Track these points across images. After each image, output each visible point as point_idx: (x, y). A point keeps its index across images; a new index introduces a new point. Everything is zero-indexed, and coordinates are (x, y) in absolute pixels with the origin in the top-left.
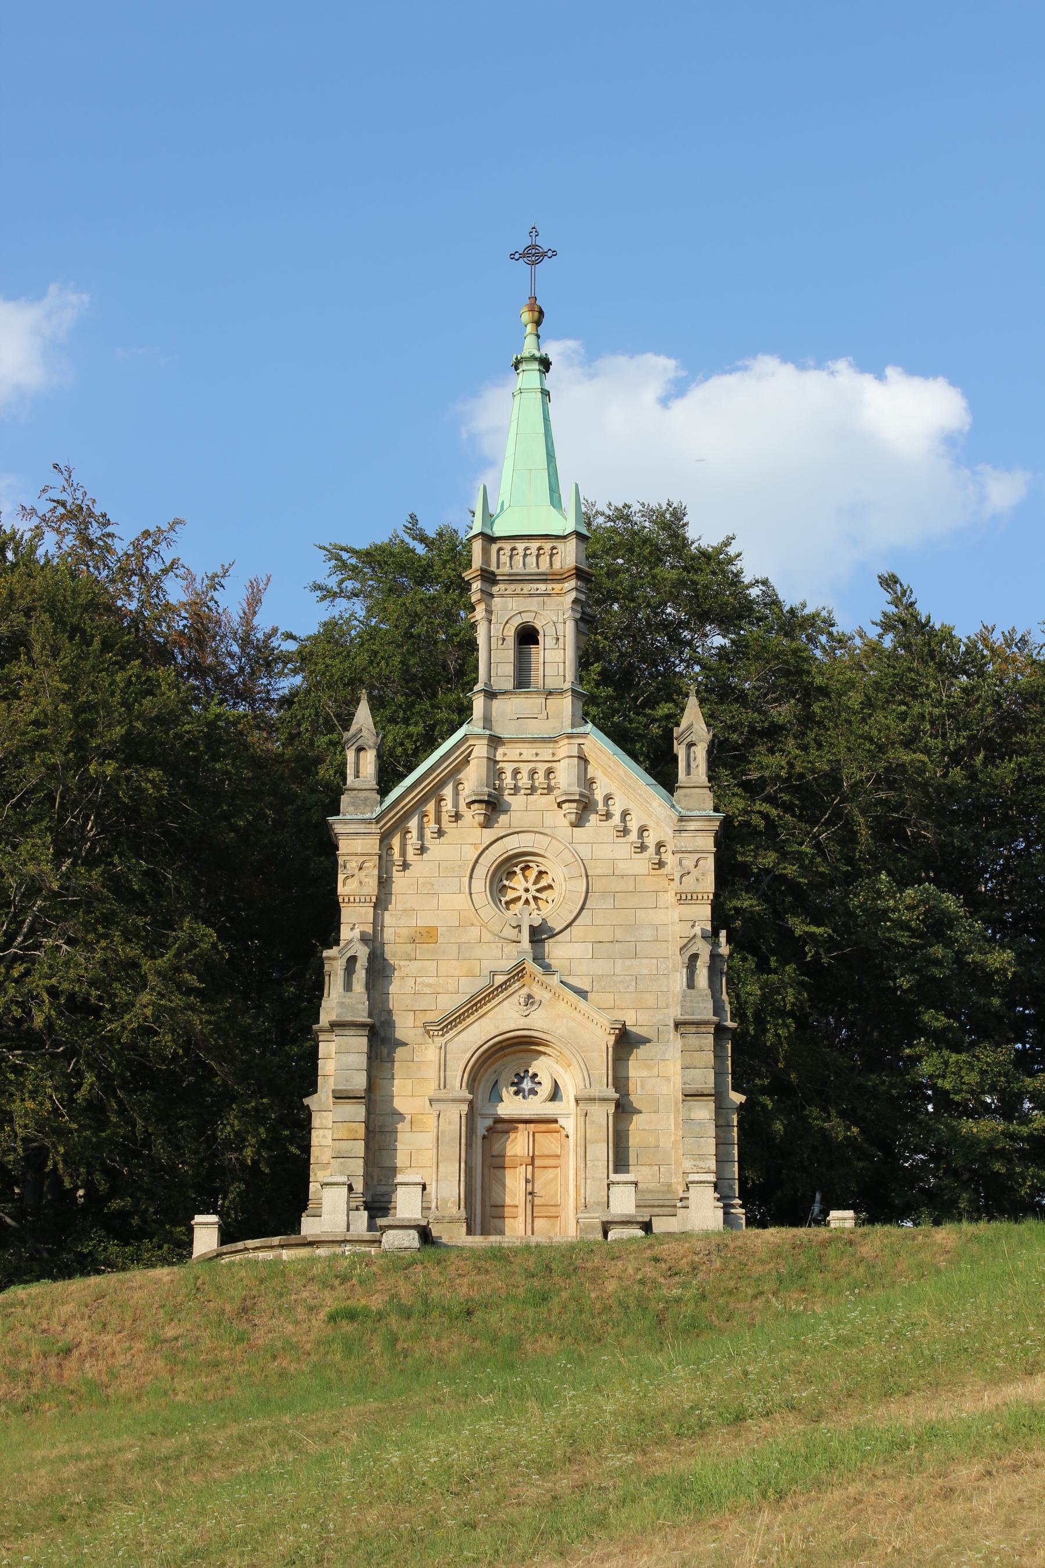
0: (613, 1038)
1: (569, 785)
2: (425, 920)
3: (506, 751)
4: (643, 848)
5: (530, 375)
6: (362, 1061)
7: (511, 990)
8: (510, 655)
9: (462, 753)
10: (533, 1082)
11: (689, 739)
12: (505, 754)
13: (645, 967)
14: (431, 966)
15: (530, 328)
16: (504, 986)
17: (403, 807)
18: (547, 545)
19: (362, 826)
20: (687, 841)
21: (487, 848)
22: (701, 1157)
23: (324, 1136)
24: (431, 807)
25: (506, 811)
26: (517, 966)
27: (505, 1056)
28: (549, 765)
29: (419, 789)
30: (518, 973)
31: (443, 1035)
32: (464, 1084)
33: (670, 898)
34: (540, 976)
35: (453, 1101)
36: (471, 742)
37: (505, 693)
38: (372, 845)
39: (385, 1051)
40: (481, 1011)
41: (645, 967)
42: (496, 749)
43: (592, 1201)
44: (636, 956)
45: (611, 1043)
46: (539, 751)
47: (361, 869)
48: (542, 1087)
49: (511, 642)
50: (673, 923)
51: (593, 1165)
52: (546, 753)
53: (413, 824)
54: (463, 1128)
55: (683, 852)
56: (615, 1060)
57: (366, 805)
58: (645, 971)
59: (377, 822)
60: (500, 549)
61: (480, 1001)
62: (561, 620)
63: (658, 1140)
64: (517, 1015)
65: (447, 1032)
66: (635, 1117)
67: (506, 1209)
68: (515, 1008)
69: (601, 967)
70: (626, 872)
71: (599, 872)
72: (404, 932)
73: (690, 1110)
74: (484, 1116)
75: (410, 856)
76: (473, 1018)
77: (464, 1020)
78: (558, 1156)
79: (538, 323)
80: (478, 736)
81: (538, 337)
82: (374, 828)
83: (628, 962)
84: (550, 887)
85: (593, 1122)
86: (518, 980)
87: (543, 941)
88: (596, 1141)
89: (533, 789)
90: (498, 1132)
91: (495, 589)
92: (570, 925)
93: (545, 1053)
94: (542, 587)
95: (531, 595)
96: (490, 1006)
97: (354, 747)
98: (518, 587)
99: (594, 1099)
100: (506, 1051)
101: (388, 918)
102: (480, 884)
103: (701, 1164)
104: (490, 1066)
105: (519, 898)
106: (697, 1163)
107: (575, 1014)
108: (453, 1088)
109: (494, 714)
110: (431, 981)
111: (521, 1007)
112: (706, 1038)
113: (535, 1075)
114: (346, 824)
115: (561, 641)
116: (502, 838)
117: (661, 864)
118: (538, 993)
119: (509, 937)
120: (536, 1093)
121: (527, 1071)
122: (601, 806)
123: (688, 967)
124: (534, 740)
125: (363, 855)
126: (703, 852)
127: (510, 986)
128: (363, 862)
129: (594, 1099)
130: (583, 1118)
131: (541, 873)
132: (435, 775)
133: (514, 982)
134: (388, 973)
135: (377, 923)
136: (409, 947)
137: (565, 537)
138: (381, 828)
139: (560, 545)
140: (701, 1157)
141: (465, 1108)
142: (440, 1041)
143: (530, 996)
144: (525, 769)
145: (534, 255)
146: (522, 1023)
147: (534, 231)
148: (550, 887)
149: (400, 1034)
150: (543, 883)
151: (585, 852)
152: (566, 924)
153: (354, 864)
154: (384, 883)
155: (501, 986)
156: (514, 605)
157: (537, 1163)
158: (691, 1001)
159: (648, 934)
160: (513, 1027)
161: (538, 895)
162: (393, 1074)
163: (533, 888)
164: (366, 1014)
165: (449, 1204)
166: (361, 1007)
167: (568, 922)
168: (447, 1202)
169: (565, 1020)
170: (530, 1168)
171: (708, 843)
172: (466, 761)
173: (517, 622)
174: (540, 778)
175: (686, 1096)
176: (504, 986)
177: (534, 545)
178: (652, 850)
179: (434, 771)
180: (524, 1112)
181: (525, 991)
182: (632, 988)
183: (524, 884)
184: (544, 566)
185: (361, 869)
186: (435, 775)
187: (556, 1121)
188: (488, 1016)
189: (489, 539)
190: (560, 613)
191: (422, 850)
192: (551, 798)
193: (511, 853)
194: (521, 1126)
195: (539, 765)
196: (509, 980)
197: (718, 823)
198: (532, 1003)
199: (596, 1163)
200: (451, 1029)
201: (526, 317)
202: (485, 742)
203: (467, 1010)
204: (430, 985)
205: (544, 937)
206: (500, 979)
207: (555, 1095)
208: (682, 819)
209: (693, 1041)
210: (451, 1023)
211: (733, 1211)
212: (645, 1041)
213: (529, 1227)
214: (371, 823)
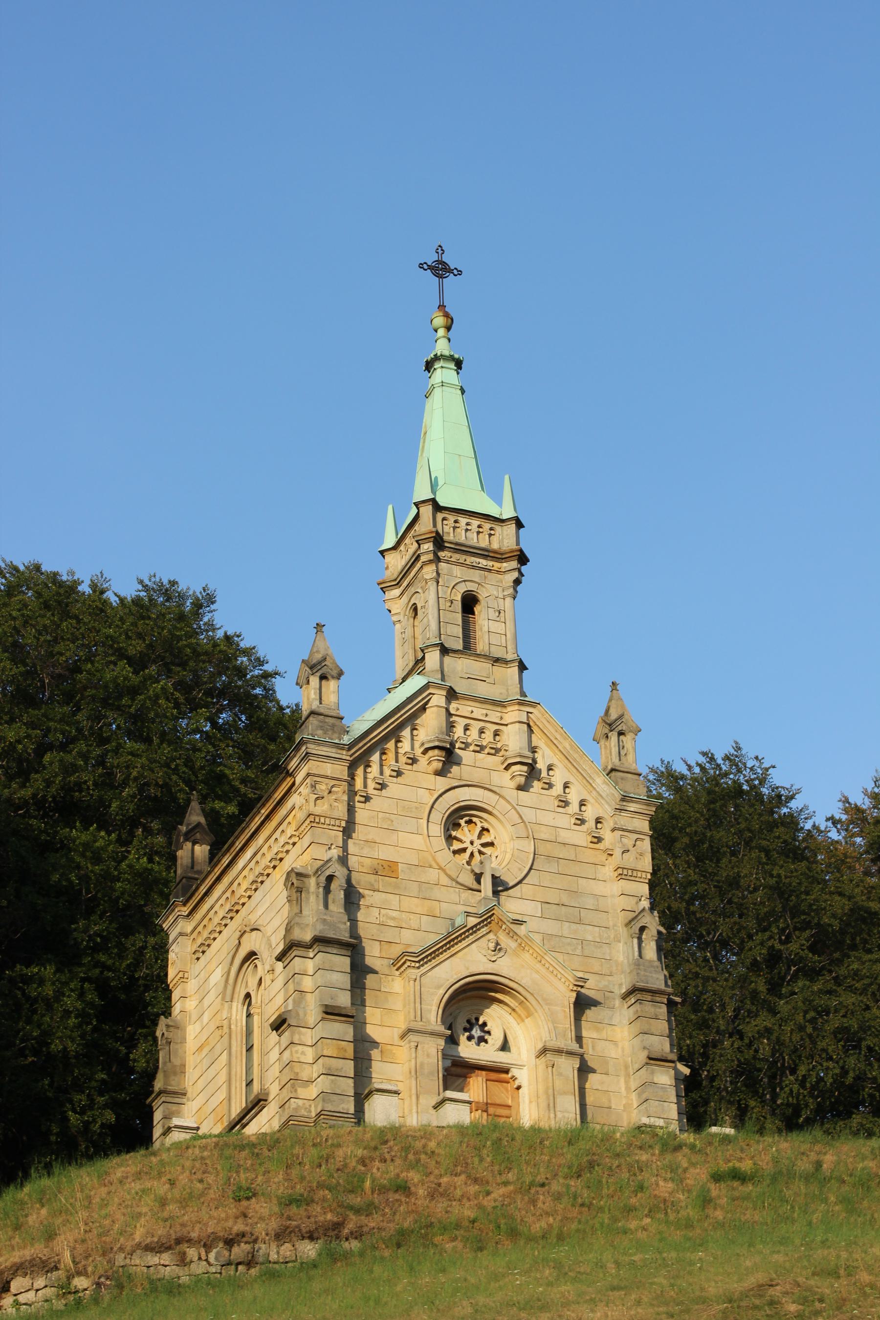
0: (574, 995)
1: (520, 748)
2: (385, 854)
3: (460, 707)
4: (582, 822)
5: (444, 373)
6: (344, 980)
7: (480, 933)
8: (459, 617)
9: (423, 699)
10: (483, 1031)
11: (620, 728)
13: (590, 933)
14: (394, 900)
15: (441, 332)
16: (474, 929)
18: (487, 526)
19: (334, 750)
21: (441, 796)
23: (303, 1053)
24: (391, 745)
25: (459, 764)
26: (489, 911)
28: (497, 727)
29: (386, 725)
30: (487, 919)
31: (418, 968)
32: (439, 1019)
33: (608, 871)
34: (508, 924)
36: (431, 691)
37: (455, 651)
38: (341, 771)
41: (590, 933)
44: (580, 922)
46: (489, 712)
47: (330, 792)
49: (458, 606)
50: (613, 896)
52: (494, 716)
53: (375, 757)
55: (623, 830)
56: (575, 1019)
57: (334, 732)
58: (590, 938)
59: (349, 749)
60: (444, 519)
61: (453, 940)
62: (501, 596)
63: (610, 1101)
64: (485, 960)
66: (591, 1076)
68: (484, 952)
70: (567, 841)
71: (543, 836)
72: (367, 862)
73: (653, 1073)
78: (509, 1107)
79: (448, 328)
80: (438, 686)
81: (449, 340)
82: (345, 755)
83: (574, 926)
84: (492, 844)
85: (560, 1074)
86: (486, 925)
88: (565, 1093)
89: (481, 749)
91: (441, 554)
92: (520, 882)
93: (500, 1002)
94: (483, 562)
95: (473, 567)
97: (318, 674)
98: (462, 558)
100: (469, 994)
102: (437, 829)
105: (464, 850)
107: (538, 966)
108: (429, 1021)
110: (394, 914)
111: (490, 952)
112: (660, 1008)
113: (485, 1024)
114: (319, 745)
115: (502, 614)
117: (599, 840)
118: (506, 941)
119: (466, 884)
120: (486, 1042)
121: (477, 1019)
122: (544, 774)
127: (479, 929)
128: (332, 787)
129: (562, 1052)
131: (484, 829)
132: (399, 715)
133: (483, 927)
135: (345, 848)
136: (372, 878)
137: (503, 521)
138: (351, 756)
139: (498, 529)
142: (414, 973)
143: (497, 944)
144: (475, 726)
145: (441, 269)
146: (490, 967)
147: (440, 249)
148: (492, 844)
149: (369, 961)
150: (486, 839)
151: (529, 815)
153: (323, 787)
154: (351, 810)
155: (472, 928)
156: (457, 571)
157: (491, 1110)
158: (645, 970)
159: (590, 903)
160: (482, 970)
161: (482, 849)
163: (477, 843)
164: (347, 935)
166: (342, 926)
171: (644, 825)
172: (423, 709)
173: (462, 588)
174: (488, 737)
175: (651, 1059)
176: (474, 929)
177: (475, 523)
178: (591, 824)
179: (399, 711)
180: (481, 1058)
181: (491, 936)
182: (578, 952)
183: (475, 837)
184: (484, 542)
185: (330, 792)
186: (399, 715)
187: (507, 1071)
189: (437, 508)
190: (500, 589)
192: (497, 759)
193: (462, 804)
195: (488, 725)
196: (479, 923)
197: (654, 809)
198: (500, 950)
201: (439, 321)
202: (444, 693)
203: (442, 947)
204: (393, 919)
206: (472, 921)
207: (505, 1047)
208: (624, 799)
209: (649, 1008)
210: (427, 957)
212: (594, 1003)
214: (342, 749)
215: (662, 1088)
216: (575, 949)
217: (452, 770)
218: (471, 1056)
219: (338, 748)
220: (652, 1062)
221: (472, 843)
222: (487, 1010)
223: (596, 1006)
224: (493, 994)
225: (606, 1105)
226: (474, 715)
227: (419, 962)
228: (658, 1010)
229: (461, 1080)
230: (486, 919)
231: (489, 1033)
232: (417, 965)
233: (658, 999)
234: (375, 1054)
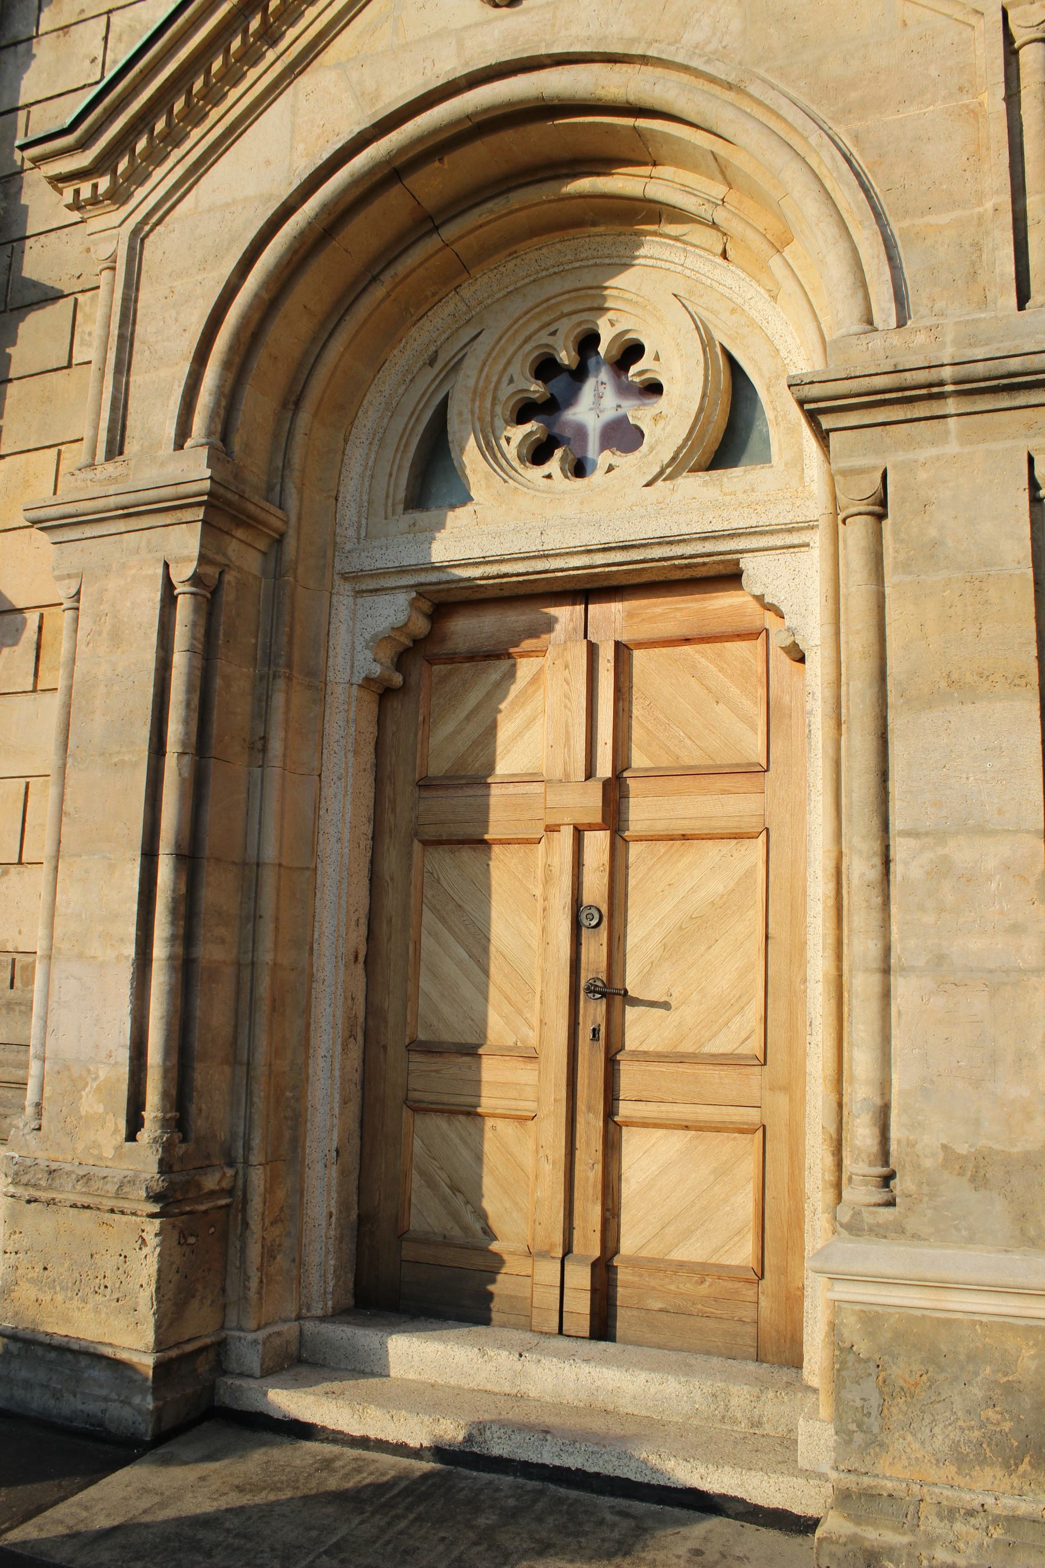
10: (625, 390)
31: (118, 196)
35: (128, 512)
43: (930, 1141)
48: (661, 404)
51: (941, 870)
54: (179, 660)
65: (138, 176)
67: (487, 1063)
77: (213, 96)
90: (452, 658)
99: (933, 392)
113: (633, 351)
129: (933, 392)
130: (856, 533)
165: (90, 1104)
170: (597, 843)
180: (554, 541)
194: (566, 615)
200: (155, 156)
213: (589, 1174)
218: (495, 549)
222: (621, 281)
224: (585, 184)
227: (103, 164)
229: (496, 671)
231: (654, 389)
232: (104, 183)
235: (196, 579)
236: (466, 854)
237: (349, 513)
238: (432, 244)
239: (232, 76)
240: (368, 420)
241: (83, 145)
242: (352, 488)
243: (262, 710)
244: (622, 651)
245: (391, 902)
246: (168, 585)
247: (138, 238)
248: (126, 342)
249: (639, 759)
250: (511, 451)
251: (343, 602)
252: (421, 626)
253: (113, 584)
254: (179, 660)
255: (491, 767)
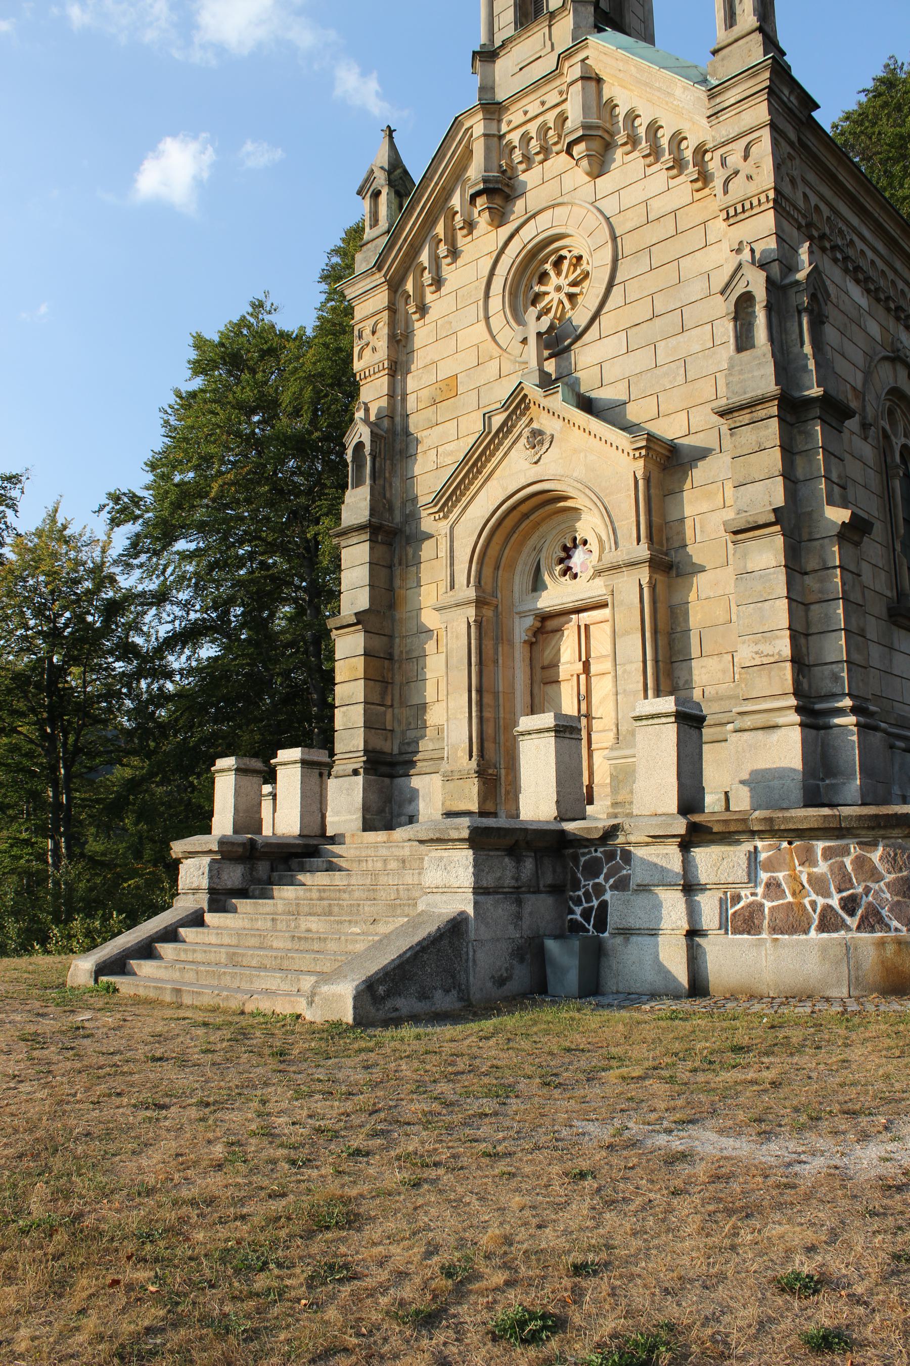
0: (641, 462)
3: (511, 117)
7: (516, 432)
12: (510, 122)
16: (506, 428)
17: (405, 240)
19: (368, 280)
20: (729, 127)
22: (767, 634)
27: (538, 525)
35: (457, 605)
36: (467, 125)
39: (410, 551)
40: (486, 471)
42: (500, 121)
45: (640, 475)
51: (625, 671)
58: (696, 348)
59: (379, 270)
65: (450, 511)
69: (642, 360)
71: (629, 226)
72: (425, 394)
73: (745, 556)
74: (522, 615)
75: (429, 297)
76: (478, 483)
82: (379, 278)
83: (673, 341)
86: (523, 414)
87: (568, 349)
88: (627, 633)
89: (545, 151)
90: (547, 633)
96: (495, 460)
101: (411, 383)
103: (767, 648)
104: (522, 543)
106: (761, 647)
109: (497, 78)
112: (767, 427)
113: (585, 542)
116: (517, 231)
121: (575, 539)
123: (735, 319)
124: (536, 85)
125: (374, 315)
126: (752, 131)
127: (513, 426)
129: (619, 567)
133: (518, 419)
134: (412, 451)
138: (385, 276)
140: (767, 634)
141: (471, 612)
146: (533, 473)
151: (609, 206)
152: (590, 315)
157: (594, 669)
160: (523, 482)
162: (419, 580)
164: (367, 513)
165: (460, 754)
167: (593, 309)
168: (457, 750)
169: (582, 455)
170: (583, 677)
175: (736, 533)
176: (506, 428)
182: (681, 379)
185: (374, 333)
188: (495, 476)
191: (438, 282)
194: (574, 617)
196: (509, 417)
198: (541, 443)
199: (628, 667)
200: (454, 506)
205: (566, 343)
206: (497, 421)
208: (713, 93)
209: (749, 437)
211: (838, 721)
212: (703, 454)
215: (761, 577)
216: (675, 378)
217: (515, 209)
218: (551, 603)
219: (368, 276)
220: (740, 537)
221: (559, 289)
223: (704, 457)
224: (562, 504)
225: (721, 621)
226: (529, 116)
228: (763, 433)
230: (518, 406)
232: (441, 514)
233: (762, 414)
234: (430, 647)
235: (475, 621)
236: (554, 685)
237: (516, 595)
238: (527, 522)
239: (471, 483)
240: (519, 568)
241: (435, 506)
242: (516, 588)
243: (496, 653)
244: (587, 627)
245: (537, 701)
246: (469, 623)
247: (452, 528)
248: (452, 557)
249: (592, 655)
250: (557, 573)
251: (517, 619)
252: (538, 624)
253: (455, 624)
254: (473, 642)
255: (559, 661)
